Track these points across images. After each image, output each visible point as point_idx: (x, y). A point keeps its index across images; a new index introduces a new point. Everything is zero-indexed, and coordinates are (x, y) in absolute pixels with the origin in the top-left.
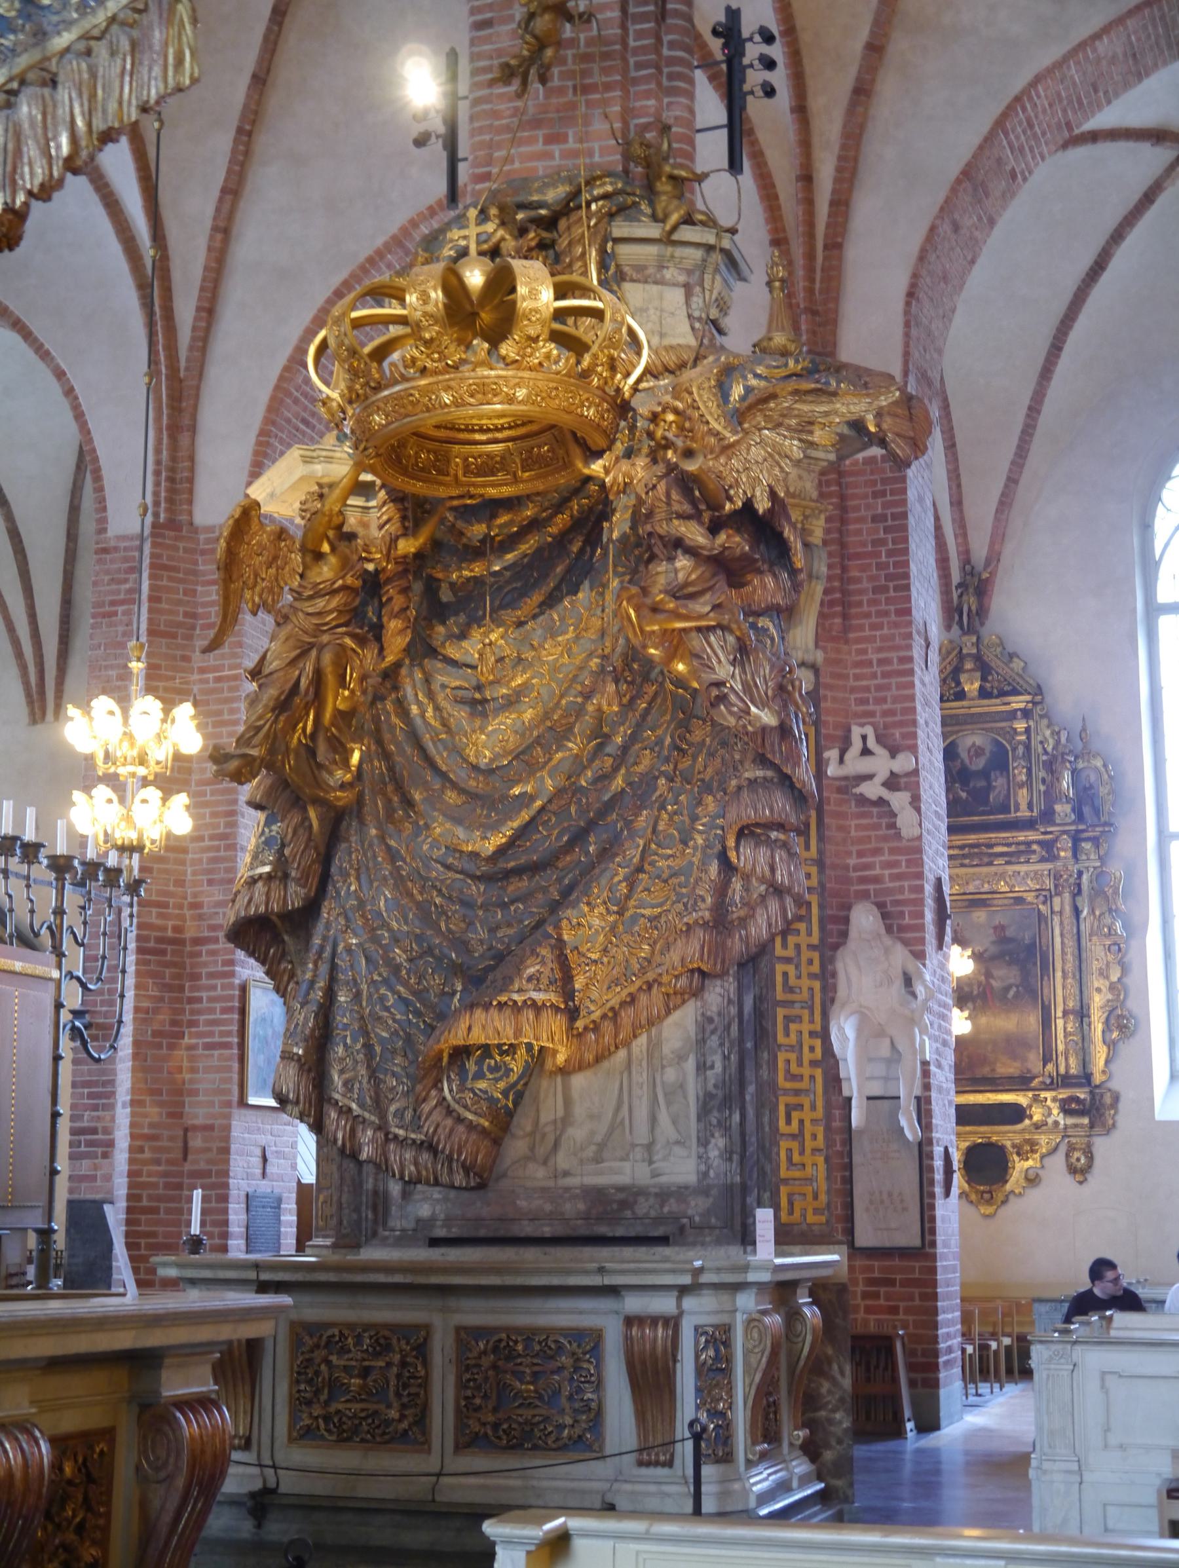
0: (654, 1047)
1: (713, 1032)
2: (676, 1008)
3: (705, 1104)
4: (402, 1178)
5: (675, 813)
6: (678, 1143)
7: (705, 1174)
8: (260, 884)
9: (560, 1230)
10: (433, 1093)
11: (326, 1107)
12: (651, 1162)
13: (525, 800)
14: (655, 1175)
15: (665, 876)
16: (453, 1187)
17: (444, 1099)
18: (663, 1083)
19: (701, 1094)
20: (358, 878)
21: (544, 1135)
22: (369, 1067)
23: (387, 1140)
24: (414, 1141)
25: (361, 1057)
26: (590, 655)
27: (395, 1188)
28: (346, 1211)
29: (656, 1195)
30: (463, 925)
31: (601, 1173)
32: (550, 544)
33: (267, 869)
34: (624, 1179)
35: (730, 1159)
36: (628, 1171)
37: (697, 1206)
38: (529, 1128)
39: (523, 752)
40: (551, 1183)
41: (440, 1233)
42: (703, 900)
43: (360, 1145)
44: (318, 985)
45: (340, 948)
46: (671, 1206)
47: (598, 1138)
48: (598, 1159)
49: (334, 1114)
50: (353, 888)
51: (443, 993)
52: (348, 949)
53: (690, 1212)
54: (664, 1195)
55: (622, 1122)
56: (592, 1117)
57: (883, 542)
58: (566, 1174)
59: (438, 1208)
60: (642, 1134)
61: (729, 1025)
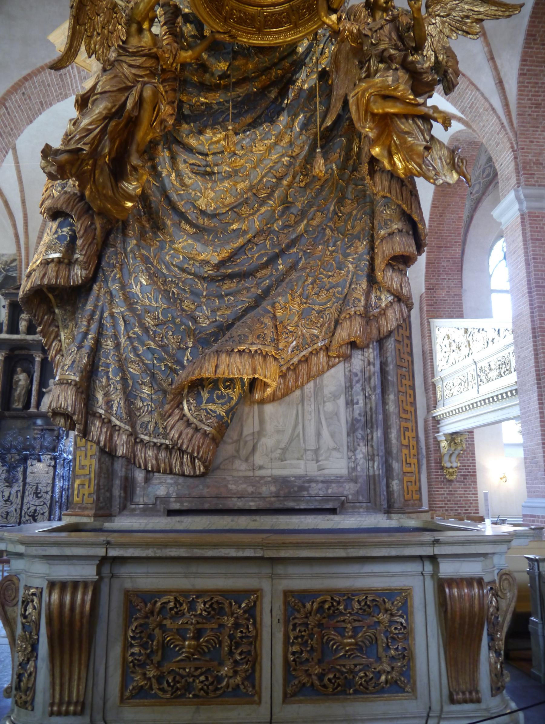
0: (318, 390)
1: (357, 382)
2: (333, 366)
3: (353, 425)
4: (146, 469)
5: (334, 251)
6: (334, 449)
7: (354, 469)
8: (52, 265)
9: (262, 505)
10: (177, 411)
11: (90, 418)
12: (317, 461)
13: (238, 233)
14: (320, 469)
15: (327, 287)
16: (183, 475)
17: (184, 415)
18: (324, 411)
19: (349, 419)
20: (121, 270)
21: (246, 442)
22: (125, 393)
23: (136, 442)
24: (155, 444)
25: (119, 387)
26: (283, 156)
27: (140, 476)
28: (102, 491)
29: (323, 482)
30: (193, 307)
31: (285, 468)
32: (255, 93)
34: (300, 471)
35: (373, 460)
36: (303, 467)
37: (349, 489)
38: (235, 438)
39: (235, 207)
40: (250, 474)
41: (176, 506)
42: (359, 301)
43: (116, 445)
44: (90, 336)
45: (106, 314)
46: (333, 489)
47: (282, 445)
49: (98, 423)
50: (118, 276)
51: (179, 348)
52: (112, 315)
53: (345, 493)
54: (327, 482)
55: (298, 435)
56: (278, 432)
58: (261, 468)
59: (171, 489)
60: (311, 444)
61: (370, 378)
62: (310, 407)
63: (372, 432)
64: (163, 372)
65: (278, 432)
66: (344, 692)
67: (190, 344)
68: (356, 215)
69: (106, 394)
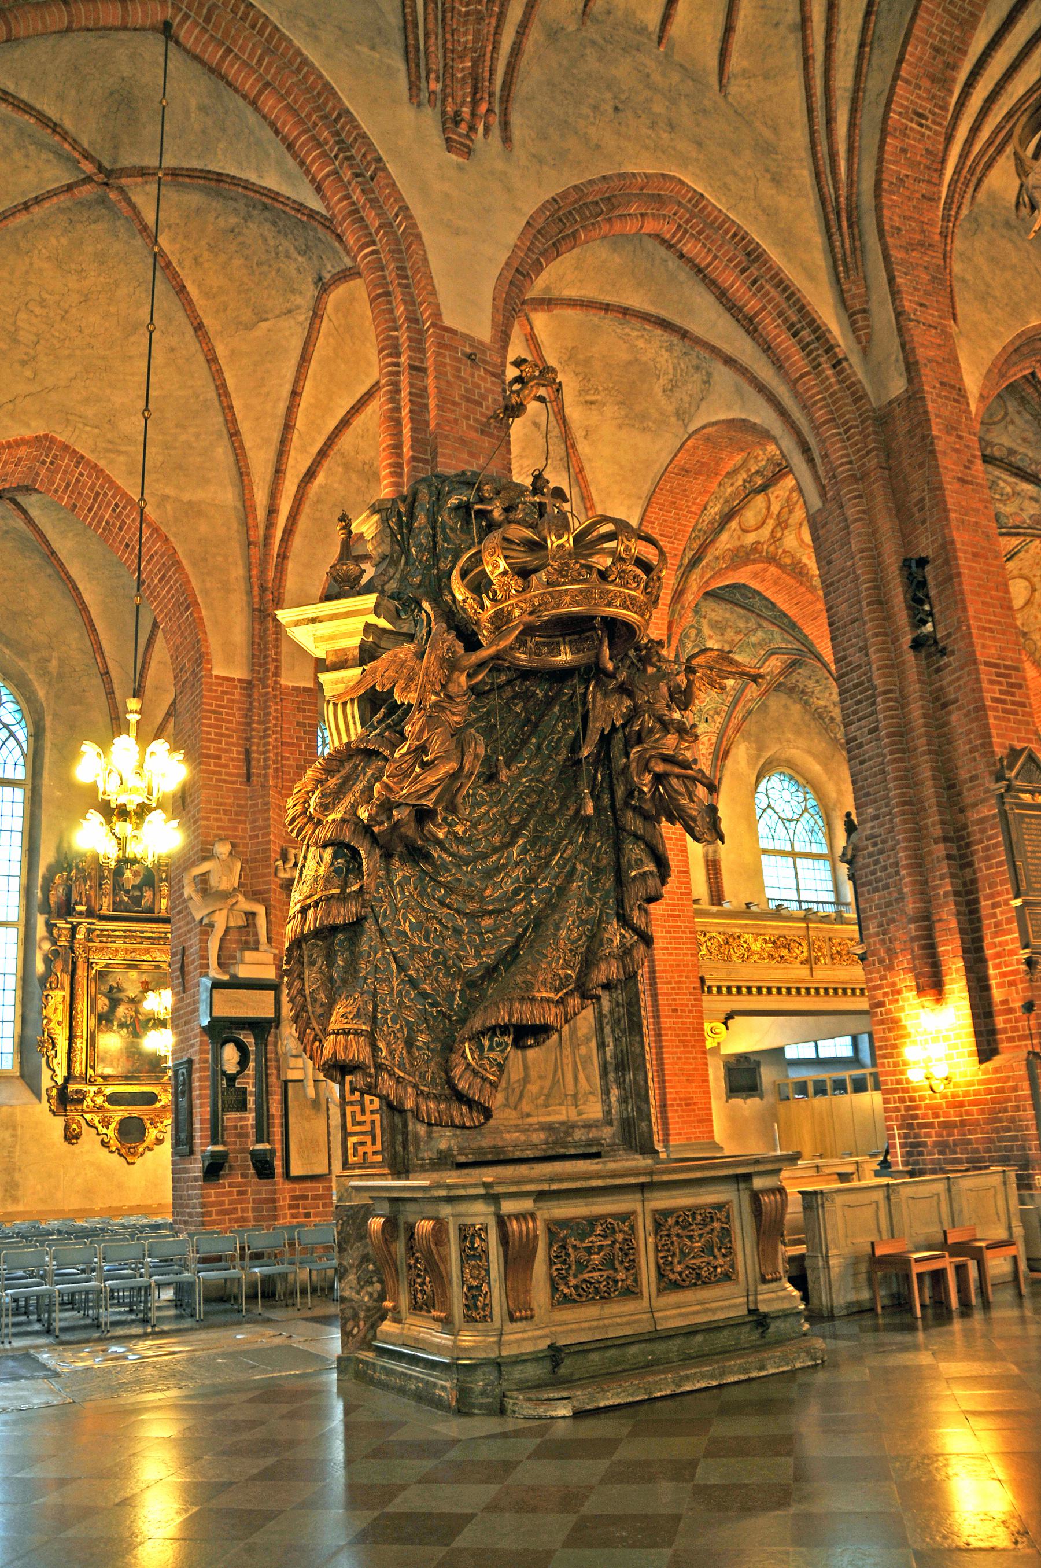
0: (573, 1031)
9: (538, 1154)
29: (584, 1127)
33: (338, 891)
34: (562, 1118)
35: (627, 1103)
37: (607, 1133)
40: (520, 1122)
41: (462, 1159)
46: (594, 1134)
47: (545, 1091)
48: (546, 1106)
54: (588, 1126)
57: (304, 739)
58: (528, 1115)
61: (619, 1020)
62: (567, 1051)
63: (624, 1075)
64: (435, 1018)
65: (540, 1077)
66: (695, 1284)
67: (459, 987)
68: (601, 847)
69: (388, 1044)
